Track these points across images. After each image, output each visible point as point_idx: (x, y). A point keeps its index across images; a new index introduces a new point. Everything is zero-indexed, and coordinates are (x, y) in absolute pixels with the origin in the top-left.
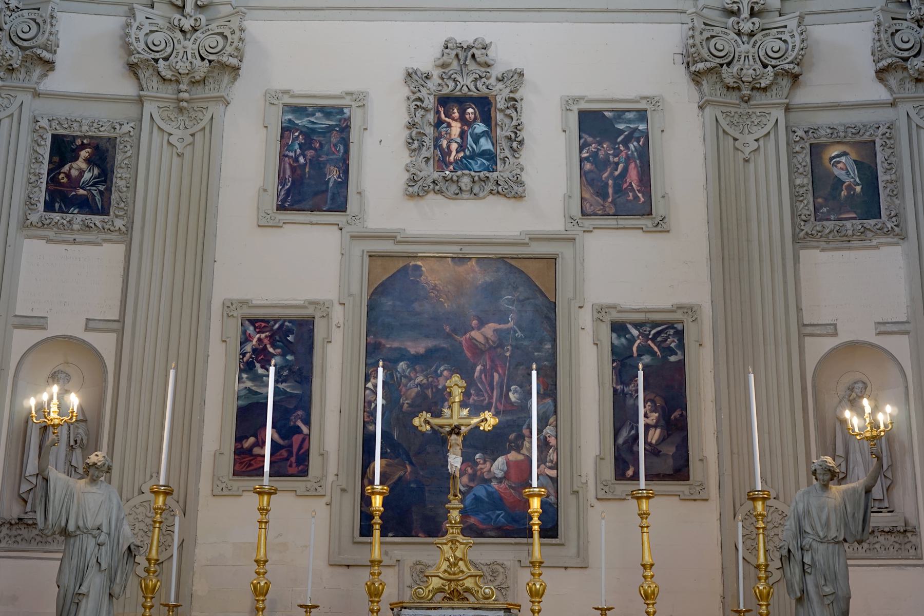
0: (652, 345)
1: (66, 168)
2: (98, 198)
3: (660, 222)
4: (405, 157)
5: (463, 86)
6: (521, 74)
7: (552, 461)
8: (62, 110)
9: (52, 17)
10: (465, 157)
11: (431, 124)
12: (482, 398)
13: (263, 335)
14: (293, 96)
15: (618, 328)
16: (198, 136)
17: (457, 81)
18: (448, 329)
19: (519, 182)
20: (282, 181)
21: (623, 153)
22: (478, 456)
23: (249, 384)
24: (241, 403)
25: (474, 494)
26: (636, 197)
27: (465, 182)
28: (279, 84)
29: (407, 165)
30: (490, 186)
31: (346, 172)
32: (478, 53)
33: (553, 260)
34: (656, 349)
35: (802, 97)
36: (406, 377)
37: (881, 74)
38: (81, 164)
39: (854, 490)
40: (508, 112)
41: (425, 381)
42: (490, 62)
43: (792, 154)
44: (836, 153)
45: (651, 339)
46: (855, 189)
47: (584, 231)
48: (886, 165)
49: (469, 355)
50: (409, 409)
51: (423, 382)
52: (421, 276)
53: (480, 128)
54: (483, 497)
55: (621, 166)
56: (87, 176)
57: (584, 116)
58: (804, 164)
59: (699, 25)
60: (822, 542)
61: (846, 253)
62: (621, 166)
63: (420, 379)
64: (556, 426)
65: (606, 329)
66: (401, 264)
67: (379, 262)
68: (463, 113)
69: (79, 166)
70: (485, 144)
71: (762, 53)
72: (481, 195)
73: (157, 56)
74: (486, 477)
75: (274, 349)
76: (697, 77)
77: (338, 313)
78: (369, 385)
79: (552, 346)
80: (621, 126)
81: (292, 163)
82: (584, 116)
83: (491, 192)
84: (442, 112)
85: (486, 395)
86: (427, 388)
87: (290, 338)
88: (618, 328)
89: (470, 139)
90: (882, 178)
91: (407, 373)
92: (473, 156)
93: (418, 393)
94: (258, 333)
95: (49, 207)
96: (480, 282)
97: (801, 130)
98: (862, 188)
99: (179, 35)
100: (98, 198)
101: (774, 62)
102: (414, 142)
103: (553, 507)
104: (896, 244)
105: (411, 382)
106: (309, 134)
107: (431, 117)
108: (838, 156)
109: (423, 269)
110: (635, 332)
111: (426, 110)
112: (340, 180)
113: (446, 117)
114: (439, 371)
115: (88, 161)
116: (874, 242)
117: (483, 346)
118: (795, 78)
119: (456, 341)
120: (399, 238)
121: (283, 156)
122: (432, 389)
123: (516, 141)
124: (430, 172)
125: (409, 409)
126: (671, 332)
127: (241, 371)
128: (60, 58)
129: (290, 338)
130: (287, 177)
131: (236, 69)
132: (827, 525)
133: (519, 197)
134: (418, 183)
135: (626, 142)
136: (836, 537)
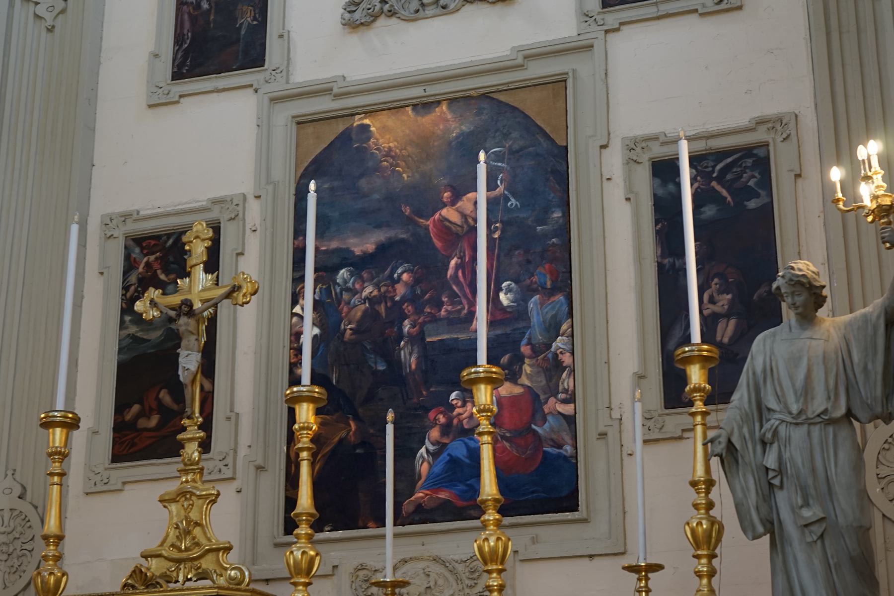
0: (718, 188)
7: (566, 391)
12: (459, 307)
13: (152, 258)
18: (407, 211)
20: (179, 39)
22: (453, 396)
23: (133, 329)
24: (124, 357)
25: (449, 455)
33: (560, 83)
34: (724, 193)
36: (348, 290)
39: (865, 318)
41: (375, 293)
45: (716, 179)
47: (607, 32)
49: (438, 243)
50: (354, 337)
51: (372, 295)
52: (369, 140)
54: (463, 458)
60: (797, 424)
63: (368, 290)
64: (572, 336)
65: (644, 174)
66: (340, 127)
67: (310, 129)
72: (452, 6)
74: (466, 427)
75: (167, 275)
77: (254, 212)
78: (297, 309)
79: (564, 213)
81: (192, 11)
85: (464, 301)
86: (379, 303)
91: (350, 285)
93: (365, 312)
94: (146, 255)
96: (454, 135)
103: (570, 462)
105: (356, 296)
109: (372, 129)
112: (255, 23)
114: (396, 275)
117: (459, 229)
119: (420, 226)
120: (336, 90)
122: (386, 303)
125: (354, 337)
126: (749, 162)
130: (185, 32)
132: (806, 392)
134: (361, 6)
136: (825, 411)
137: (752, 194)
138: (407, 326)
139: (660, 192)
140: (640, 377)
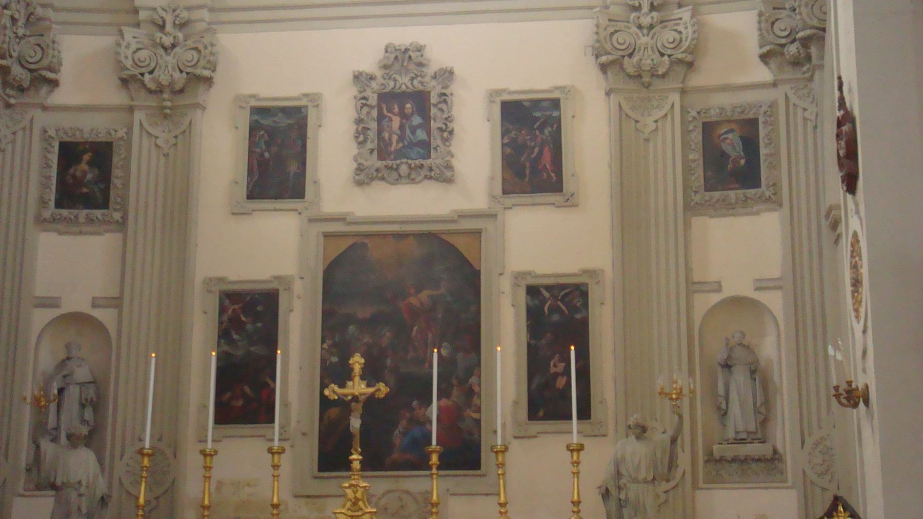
0: (561, 305)
1: (72, 171)
2: (98, 195)
3: (570, 198)
4: (354, 150)
5: (402, 84)
6: (451, 72)
7: (476, 406)
8: (67, 121)
9: (54, 42)
10: (404, 147)
11: (374, 119)
13: (236, 307)
14: (259, 100)
15: (532, 291)
16: (180, 138)
17: (396, 80)
19: (449, 167)
21: (539, 138)
23: (226, 348)
26: (549, 176)
27: (404, 169)
28: (247, 90)
29: (355, 157)
30: (424, 172)
31: (304, 164)
32: (413, 55)
33: (478, 233)
34: (564, 308)
35: (697, 80)
37: (765, 58)
38: (84, 166)
40: (440, 106)
42: (424, 62)
43: (685, 132)
44: (725, 130)
45: (560, 300)
46: (740, 162)
47: (505, 208)
48: (766, 141)
53: (417, 120)
55: (536, 150)
56: (89, 176)
57: (505, 105)
58: (696, 141)
59: (604, 22)
61: (731, 219)
62: (536, 150)
63: (366, 339)
65: (522, 292)
68: (402, 108)
69: (83, 169)
70: (421, 135)
71: (659, 44)
72: (417, 180)
73: (143, 70)
75: (246, 318)
76: (604, 68)
77: (298, 287)
80: (537, 114)
82: (505, 105)
83: (426, 177)
84: (385, 108)
87: (259, 308)
88: (532, 291)
89: (408, 132)
90: (763, 151)
92: (412, 145)
94: (233, 305)
95: (59, 204)
97: (695, 111)
98: (746, 161)
99: (161, 51)
100: (98, 195)
101: (669, 52)
102: (361, 136)
104: (774, 210)
106: (272, 132)
107: (375, 113)
108: (726, 133)
110: (546, 294)
111: (372, 107)
113: (387, 112)
115: (90, 163)
116: (755, 209)
118: (690, 65)
120: (348, 220)
121: (251, 152)
123: (447, 133)
124: (374, 162)
127: (220, 337)
128: (65, 75)
129: (259, 308)
131: (209, 81)
133: (450, 181)
134: (364, 171)
135: (541, 128)
137: (577, 310)
138: (389, 362)
139: (531, 303)
140: (516, 403)
